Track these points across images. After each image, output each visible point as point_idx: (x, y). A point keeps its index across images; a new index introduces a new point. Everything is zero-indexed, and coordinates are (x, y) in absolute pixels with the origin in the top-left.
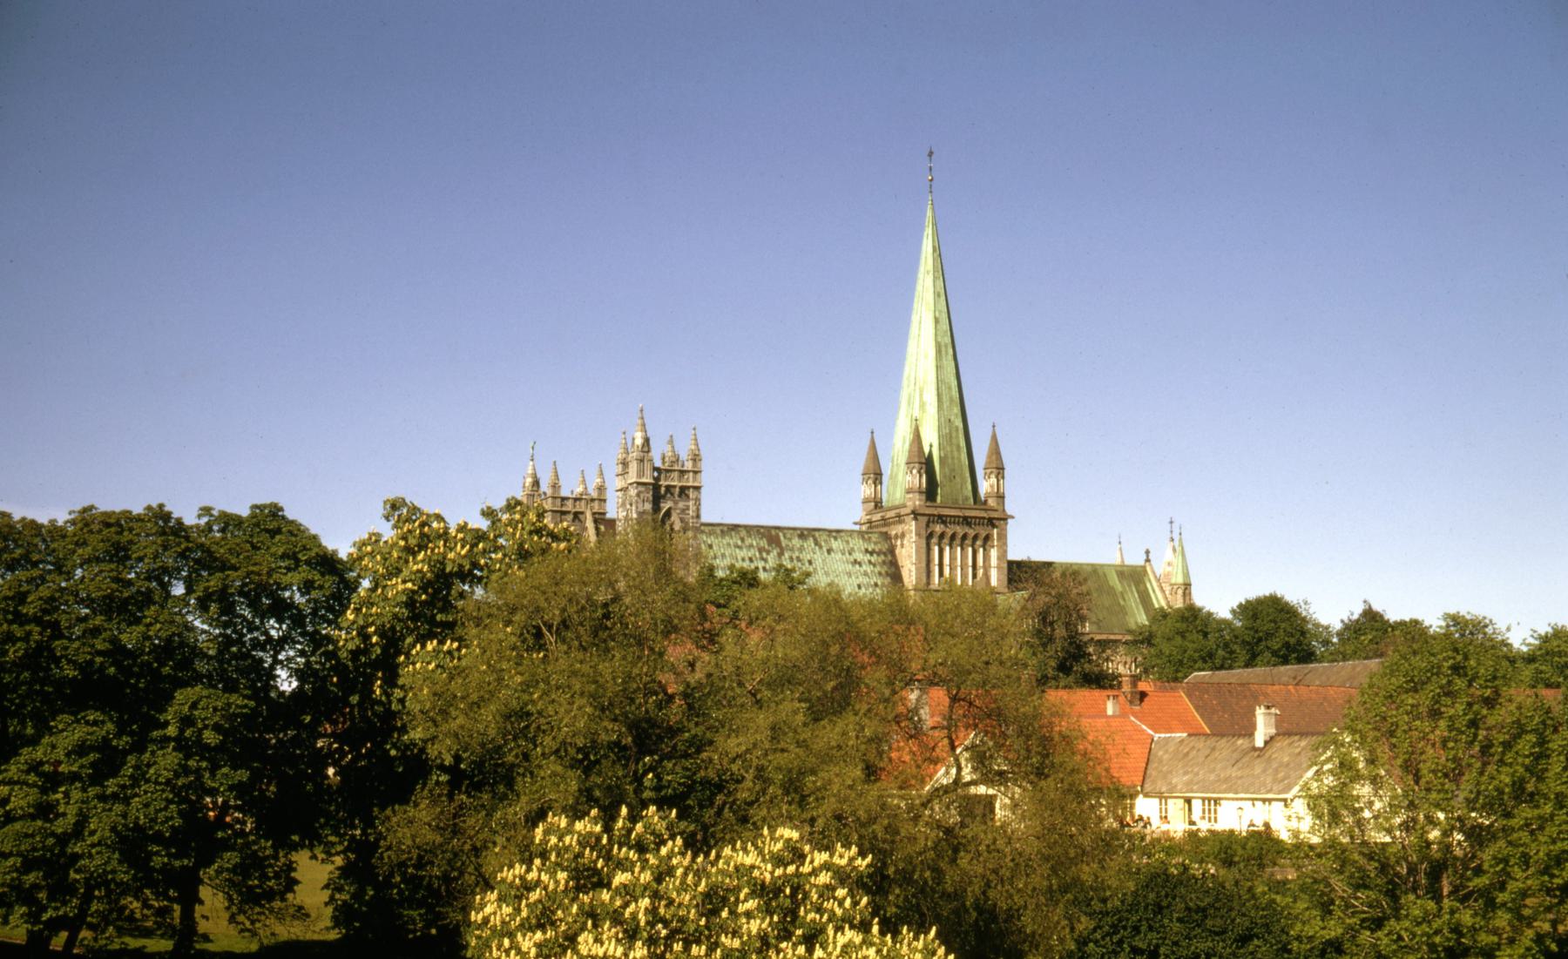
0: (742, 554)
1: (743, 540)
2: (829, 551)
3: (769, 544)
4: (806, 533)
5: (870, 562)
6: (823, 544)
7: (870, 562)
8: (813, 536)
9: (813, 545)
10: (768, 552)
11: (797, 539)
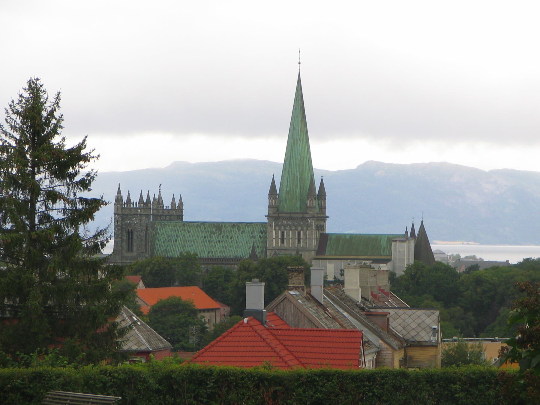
1: (205, 229)
8: (238, 226)
10: (214, 234)
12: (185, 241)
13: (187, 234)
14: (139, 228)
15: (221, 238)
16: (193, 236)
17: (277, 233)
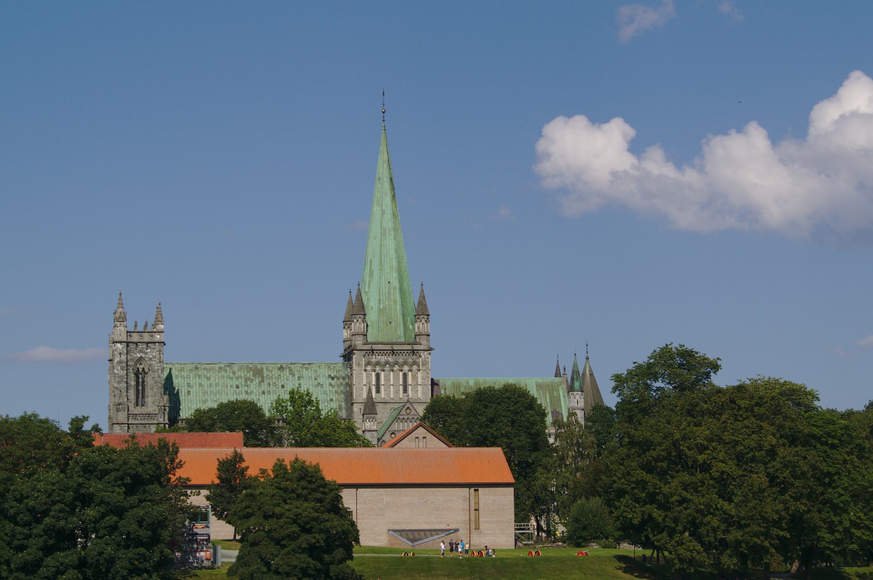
0: (231, 383)
1: (234, 373)
3: (253, 376)
4: (284, 366)
5: (330, 384)
6: (296, 373)
7: (330, 384)
8: (291, 370)
9: (288, 374)
10: (252, 381)
11: (276, 371)
12: (205, 393)
13: (205, 383)
14: (159, 365)
15: (265, 387)
16: (217, 385)
17: (369, 377)
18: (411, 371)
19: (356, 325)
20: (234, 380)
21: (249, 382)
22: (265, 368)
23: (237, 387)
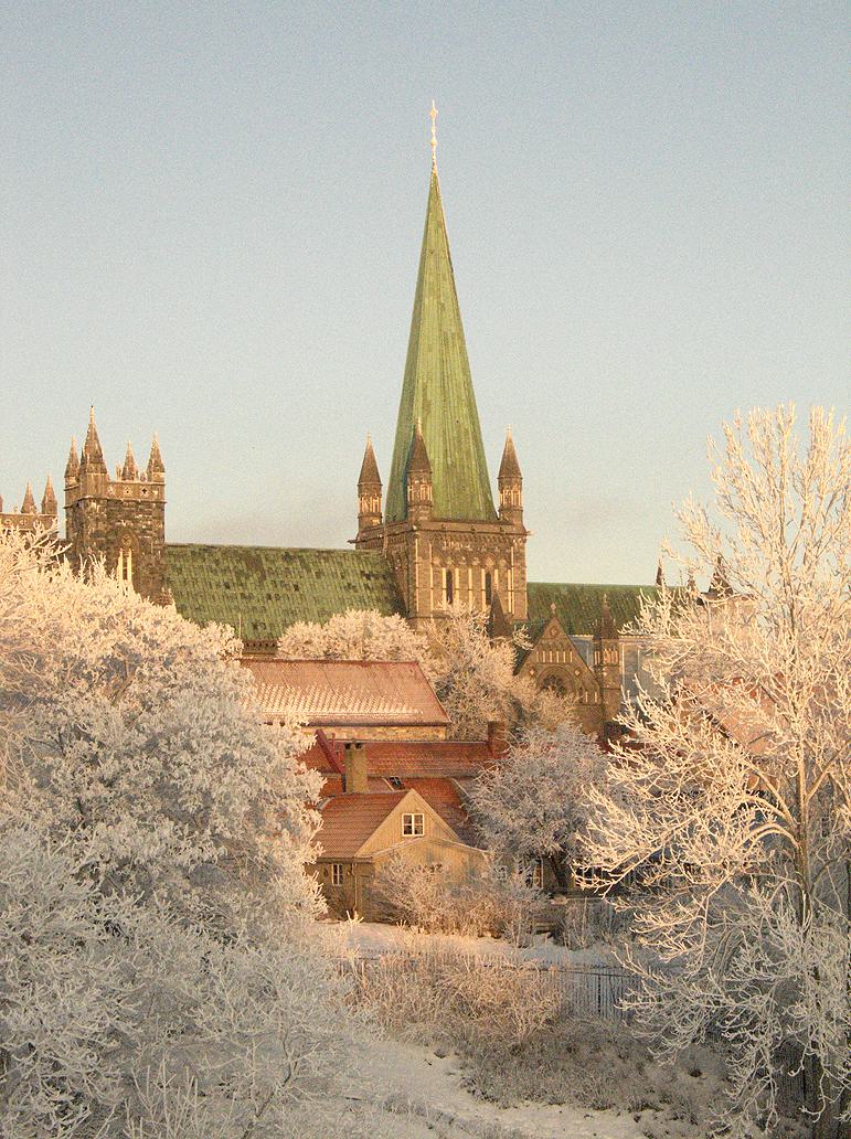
1: (217, 562)
2: (319, 574)
3: (248, 568)
7: (367, 587)
8: (302, 561)
15: (269, 588)
16: (195, 581)
17: (437, 575)
18: (496, 566)
19: (418, 488)
20: (220, 575)
21: (243, 579)
22: (262, 556)
23: (228, 587)
